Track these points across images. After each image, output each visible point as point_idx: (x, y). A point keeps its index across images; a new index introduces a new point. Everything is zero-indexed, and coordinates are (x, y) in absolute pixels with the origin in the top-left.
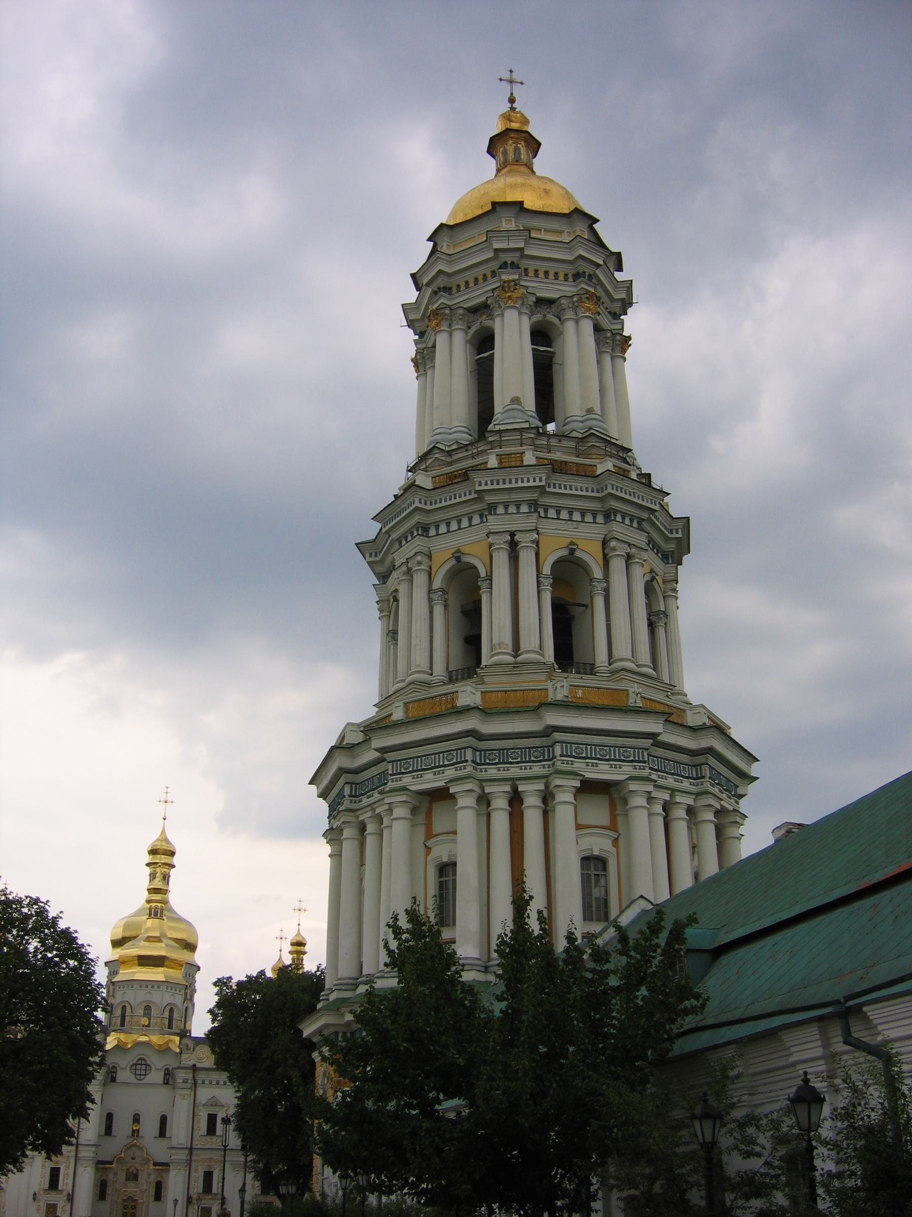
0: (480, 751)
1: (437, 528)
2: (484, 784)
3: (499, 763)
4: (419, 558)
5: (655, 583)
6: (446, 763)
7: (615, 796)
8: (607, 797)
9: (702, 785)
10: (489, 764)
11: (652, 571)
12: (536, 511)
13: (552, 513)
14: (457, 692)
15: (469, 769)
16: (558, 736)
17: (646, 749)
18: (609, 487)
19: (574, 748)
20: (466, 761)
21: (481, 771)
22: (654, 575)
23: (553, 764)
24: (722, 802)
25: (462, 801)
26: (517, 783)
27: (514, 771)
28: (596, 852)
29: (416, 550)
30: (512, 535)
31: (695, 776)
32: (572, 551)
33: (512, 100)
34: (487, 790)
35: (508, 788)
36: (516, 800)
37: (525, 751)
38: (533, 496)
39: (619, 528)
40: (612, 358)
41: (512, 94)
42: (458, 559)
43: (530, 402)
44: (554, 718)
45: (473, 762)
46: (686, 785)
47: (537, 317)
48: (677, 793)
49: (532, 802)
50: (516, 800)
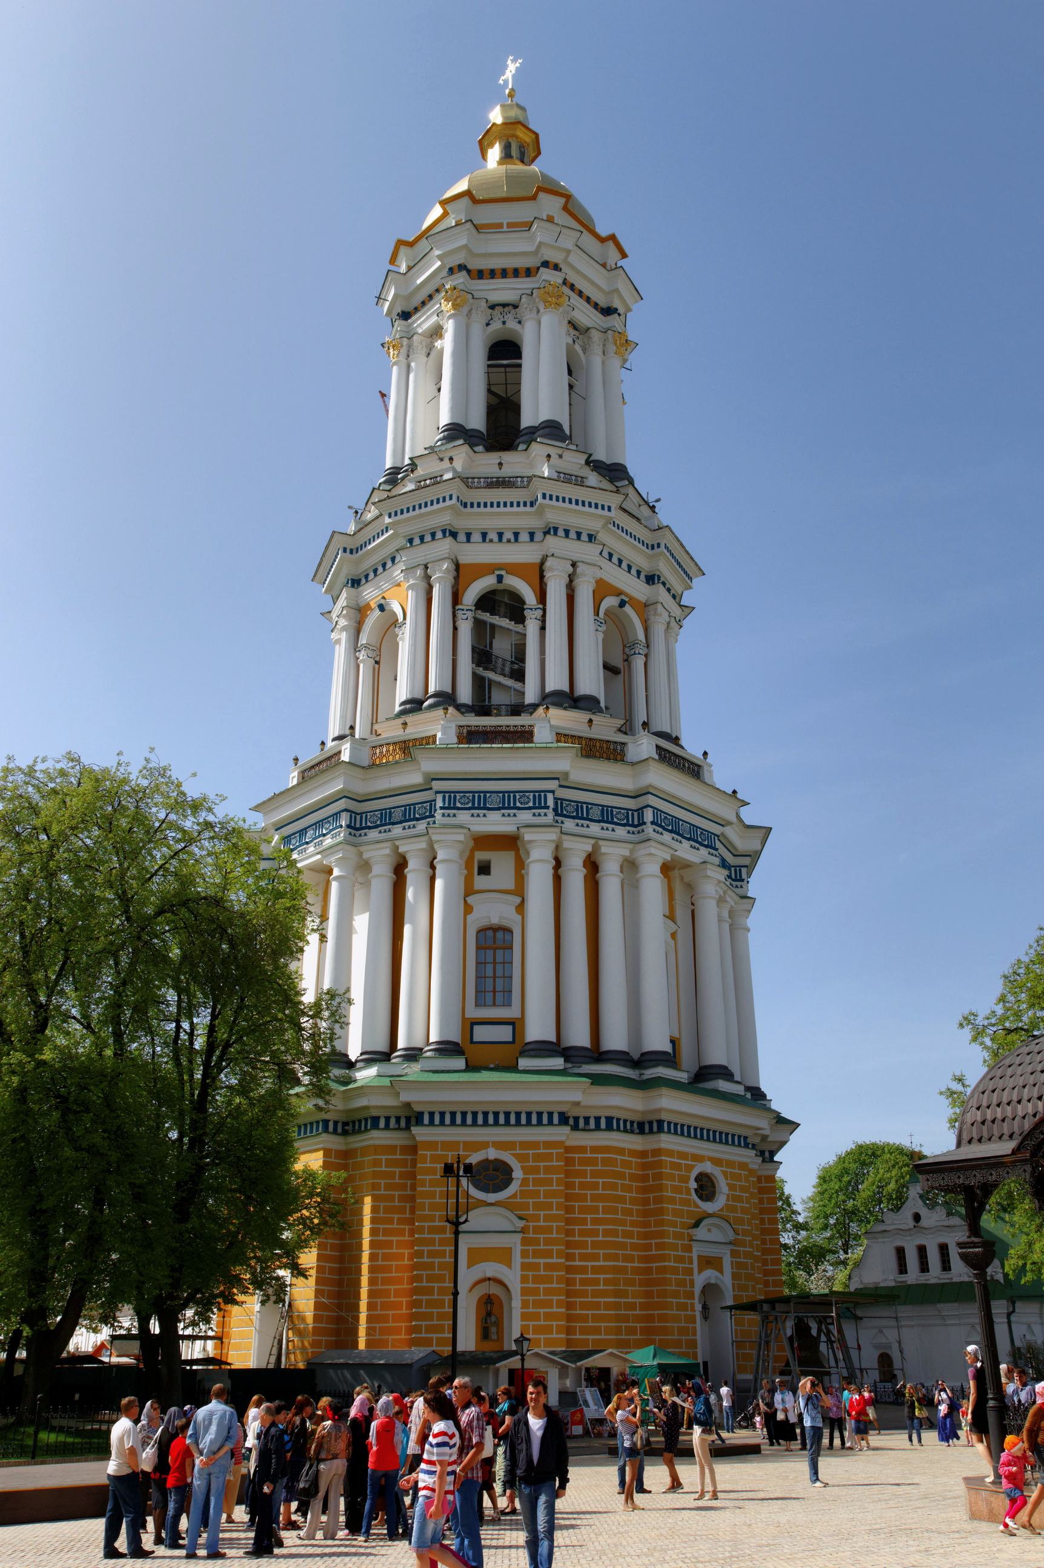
0: (361, 814)
1: (367, 576)
2: (362, 849)
4: (344, 612)
5: (628, 608)
6: (324, 832)
7: (521, 852)
8: (512, 854)
9: (643, 831)
10: (370, 828)
11: (618, 593)
12: (454, 535)
13: (476, 537)
14: (340, 752)
16: (437, 785)
17: (553, 792)
18: (540, 496)
19: (458, 798)
21: (360, 835)
22: (624, 598)
23: (434, 822)
24: (676, 853)
25: (336, 872)
26: (397, 843)
27: (397, 830)
28: (495, 921)
29: (345, 604)
30: (426, 568)
31: (636, 822)
32: (500, 579)
34: (365, 856)
35: (387, 851)
36: (400, 868)
37: (410, 809)
38: (445, 519)
39: (553, 543)
40: (603, 362)
42: (382, 608)
43: (477, 421)
44: (430, 764)
46: (621, 832)
47: (496, 325)
48: (601, 843)
49: (412, 864)
50: (400, 868)
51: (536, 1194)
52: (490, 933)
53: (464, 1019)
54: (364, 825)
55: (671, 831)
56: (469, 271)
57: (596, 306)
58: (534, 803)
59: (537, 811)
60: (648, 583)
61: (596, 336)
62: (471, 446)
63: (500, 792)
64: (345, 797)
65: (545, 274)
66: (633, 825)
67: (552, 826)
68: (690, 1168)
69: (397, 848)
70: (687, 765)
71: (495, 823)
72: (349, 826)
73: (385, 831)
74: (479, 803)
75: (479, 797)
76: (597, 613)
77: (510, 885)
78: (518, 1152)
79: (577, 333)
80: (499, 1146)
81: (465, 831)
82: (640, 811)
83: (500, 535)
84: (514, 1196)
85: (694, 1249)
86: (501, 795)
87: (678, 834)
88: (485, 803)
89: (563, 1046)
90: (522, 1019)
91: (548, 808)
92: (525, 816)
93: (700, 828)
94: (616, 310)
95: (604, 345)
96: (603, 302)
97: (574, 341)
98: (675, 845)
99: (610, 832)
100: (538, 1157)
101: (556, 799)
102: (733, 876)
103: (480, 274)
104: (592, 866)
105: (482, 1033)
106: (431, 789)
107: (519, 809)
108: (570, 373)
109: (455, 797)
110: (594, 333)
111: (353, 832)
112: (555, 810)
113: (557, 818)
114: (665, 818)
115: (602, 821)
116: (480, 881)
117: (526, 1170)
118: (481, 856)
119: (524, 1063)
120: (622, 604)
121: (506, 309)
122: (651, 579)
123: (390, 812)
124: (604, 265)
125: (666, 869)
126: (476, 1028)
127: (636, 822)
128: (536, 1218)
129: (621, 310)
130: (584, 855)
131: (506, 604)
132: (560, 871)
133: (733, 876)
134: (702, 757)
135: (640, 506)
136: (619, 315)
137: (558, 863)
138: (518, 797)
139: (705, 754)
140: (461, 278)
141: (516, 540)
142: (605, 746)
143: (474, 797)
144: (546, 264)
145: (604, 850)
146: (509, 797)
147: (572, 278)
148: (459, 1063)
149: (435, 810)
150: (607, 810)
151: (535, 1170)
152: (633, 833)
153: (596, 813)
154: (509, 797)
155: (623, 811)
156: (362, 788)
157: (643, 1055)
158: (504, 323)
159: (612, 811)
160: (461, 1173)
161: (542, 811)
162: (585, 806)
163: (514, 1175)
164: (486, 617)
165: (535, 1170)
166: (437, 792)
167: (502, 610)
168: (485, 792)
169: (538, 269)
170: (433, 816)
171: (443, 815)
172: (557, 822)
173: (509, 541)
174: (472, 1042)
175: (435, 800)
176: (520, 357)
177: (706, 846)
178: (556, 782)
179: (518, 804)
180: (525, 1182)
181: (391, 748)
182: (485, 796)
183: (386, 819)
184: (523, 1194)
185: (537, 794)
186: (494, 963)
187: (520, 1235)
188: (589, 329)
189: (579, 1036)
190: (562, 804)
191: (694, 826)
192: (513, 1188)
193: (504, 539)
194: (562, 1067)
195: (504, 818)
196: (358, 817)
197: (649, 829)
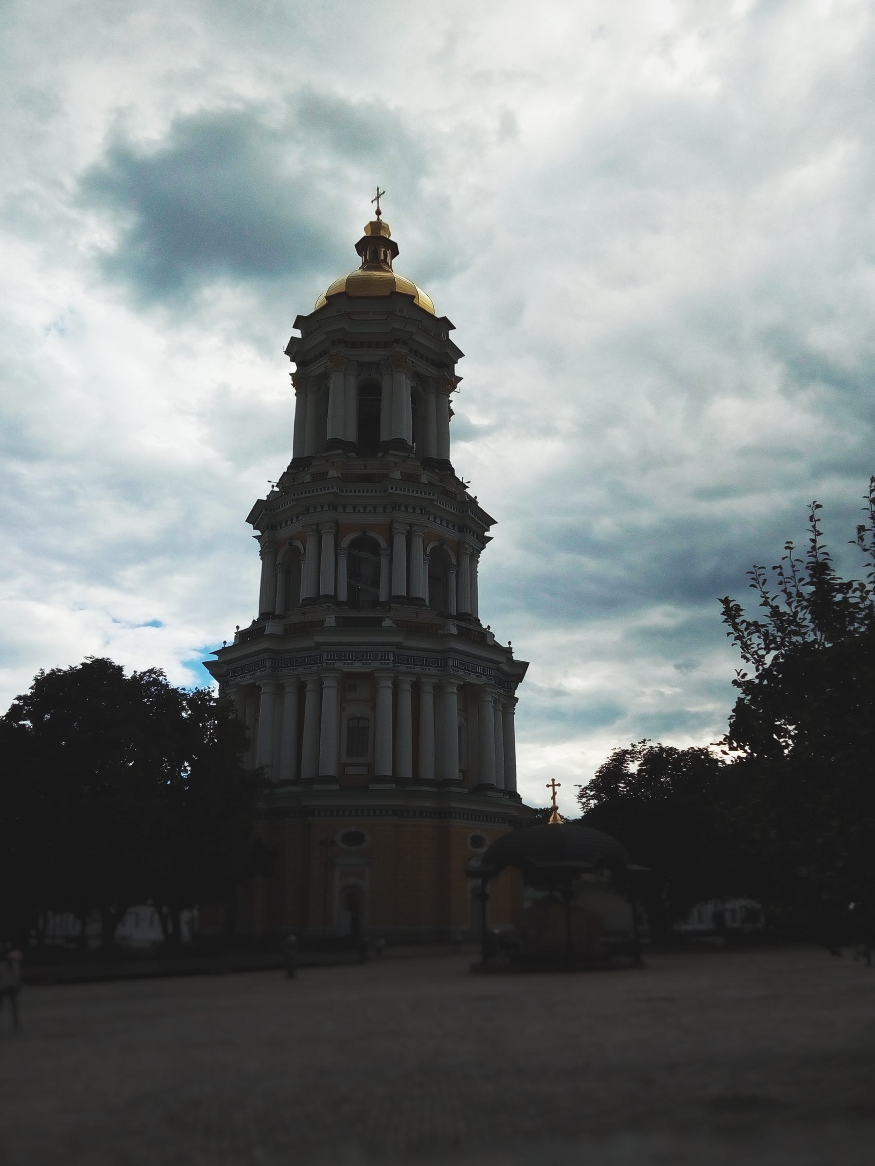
5: (445, 547)
33: (378, 213)
41: (378, 207)
46: (434, 671)
58: (382, 657)
60: (460, 531)
63: (361, 652)
66: (441, 667)
76: (425, 551)
83: (365, 508)
91: (390, 660)
92: (376, 664)
101: (395, 655)
104: (417, 689)
112: (394, 661)
115: (424, 666)
120: (442, 544)
122: (461, 529)
127: (443, 666)
139: (489, 627)
141: (375, 512)
159: (429, 660)
162: (412, 658)
172: (395, 667)
176: (381, 395)
193: (368, 511)
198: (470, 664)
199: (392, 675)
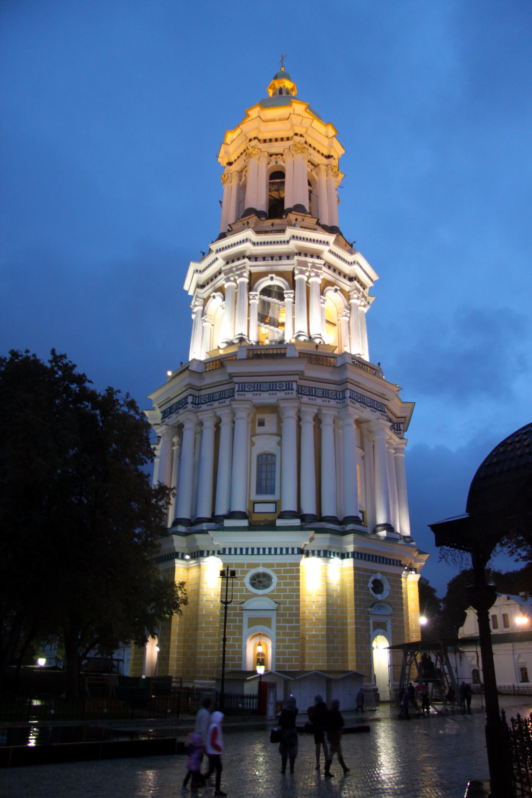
0: (198, 397)
2: (199, 414)
3: (209, 402)
6: (180, 406)
8: (276, 415)
9: (345, 402)
10: (203, 404)
15: (190, 406)
16: (235, 380)
17: (296, 381)
20: (188, 403)
25: (187, 426)
27: (216, 404)
34: (200, 417)
35: (211, 415)
37: (223, 393)
45: (192, 403)
46: (333, 403)
47: (273, 164)
51: (285, 590)
52: (264, 457)
53: (250, 501)
54: (200, 402)
55: (360, 402)
56: (259, 140)
57: (322, 154)
58: (286, 387)
59: (287, 392)
61: (323, 168)
62: (259, 217)
64: (190, 388)
65: (297, 139)
66: (340, 399)
67: (295, 399)
68: (369, 577)
69: (215, 413)
70: (369, 369)
71: (266, 398)
72: (192, 403)
73: (210, 405)
74: (257, 388)
75: (257, 385)
77: (274, 430)
78: (275, 568)
79: (313, 167)
80: (265, 565)
81: (249, 402)
82: (343, 392)
84: (273, 591)
85: (371, 619)
86: (269, 384)
87: (364, 404)
88: (260, 388)
89: (301, 514)
90: (280, 501)
91: (293, 390)
92: (281, 394)
93: (376, 401)
94: (332, 156)
95: (327, 172)
96: (326, 153)
97: (312, 170)
98: (362, 409)
99: (327, 403)
100: (286, 571)
101: (297, 385)
102: (396, 428)
103: (265, 141)
104: (318, 420)
105: (259, 508)
106: (232, 382)
107: (278, 390)
108: (310, 184)
109: (245, 385)
110: (321, 166)
111: (194, 406)
112: (296, 391)
113: (298, 395)
114: (357, 395)
116: (259, 429)
117: (279, 578)
118: (259, 416)
119: (280, 522)
121: (278, 156)
123: (213, 396)
124: (327, 137)
125: (358, 422)
126: (256, 505)
128: (285, 603)
129: (335, 156)
130: (313, 415)
131: (276, 292)
132: (301, 423)
133: (396, 428)
134: (377, 366)
135: (346, 245)
136: (334, 159)
137: (299, 419)
138: (277, 385)
139: (379, 364)
140: (255, 142)
142: (325, 359)
143: (254, 385)
144: (296, 134)
145: (324, 412)
146: (273, 385)
147: (309, 142)
148: (245, 523)
149: (234, 392)
150: (326, 391)
151: (285, 578)
152: (340, 403)
153: (320, 393)
154: (273, 385)
155: (334, 392)
156: (197, 383)
157: (345, 518)
158: (276, 162)
160: (229, 575)
161: (290, 391)
162: (313, 389)
163: (273, 580)
164: (266, 298)
165: (285, 578)
166: (236, 383)
167: (274, 294)
168: (260, 383)
169: (292, 137)
170: (233, 396)
171: (239, 395)
173: (277, 260)
174: (254, 512)
175: (235, 388)
177: (380, 411)
178: (298, 376)
179: (278, 388)
180: (279, 584)
181: (214, 363)
182: (260, 385)
183: (211, 399)
184: (278, 590)
185: (287, 383)
186: (266, 472)
187: (276, 611)
188: (319, 165)
189: (309, 508)
190: (301, 388)
191: (373, 400)
192: (273, 587)
194: (299, 524)
195: (271, 396)
196: (197, 399)
197: (348, 401)
198: (365, 398)
199: (296, 404)
